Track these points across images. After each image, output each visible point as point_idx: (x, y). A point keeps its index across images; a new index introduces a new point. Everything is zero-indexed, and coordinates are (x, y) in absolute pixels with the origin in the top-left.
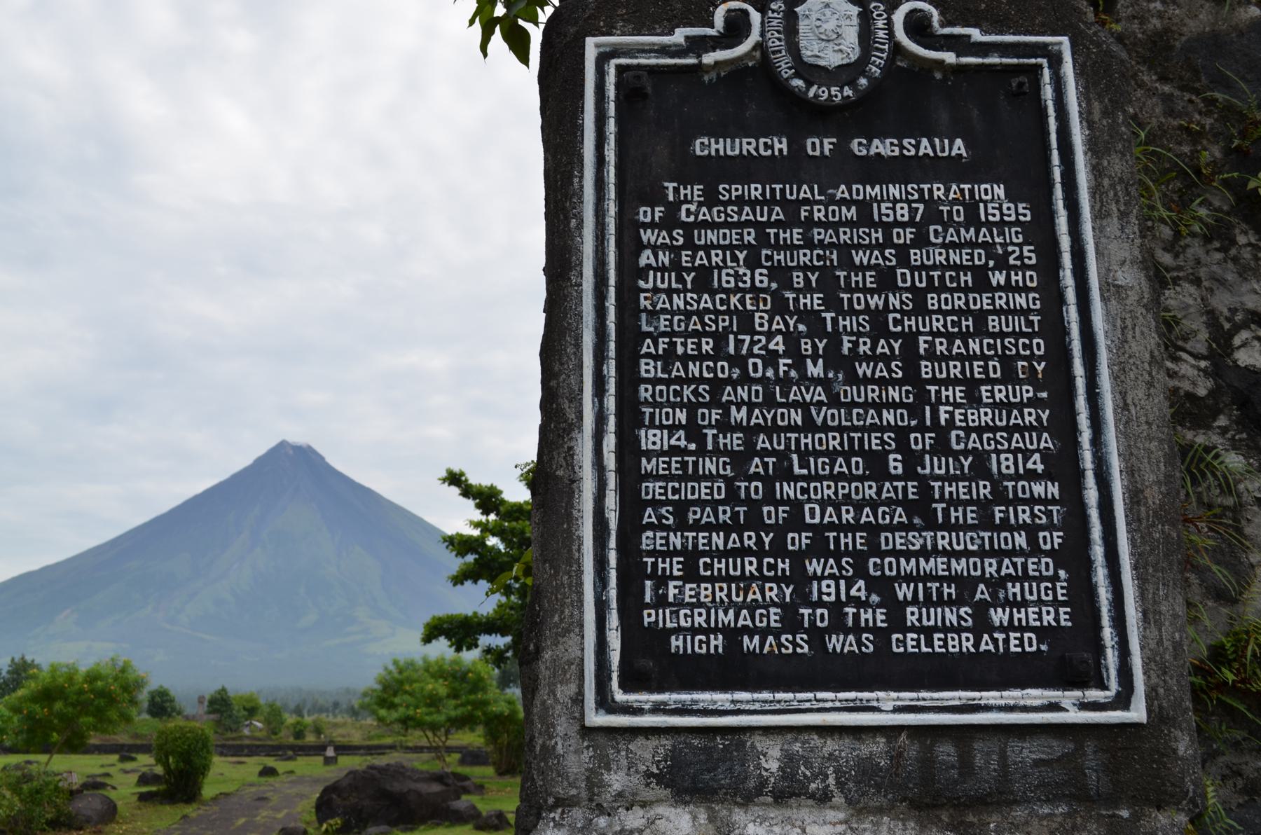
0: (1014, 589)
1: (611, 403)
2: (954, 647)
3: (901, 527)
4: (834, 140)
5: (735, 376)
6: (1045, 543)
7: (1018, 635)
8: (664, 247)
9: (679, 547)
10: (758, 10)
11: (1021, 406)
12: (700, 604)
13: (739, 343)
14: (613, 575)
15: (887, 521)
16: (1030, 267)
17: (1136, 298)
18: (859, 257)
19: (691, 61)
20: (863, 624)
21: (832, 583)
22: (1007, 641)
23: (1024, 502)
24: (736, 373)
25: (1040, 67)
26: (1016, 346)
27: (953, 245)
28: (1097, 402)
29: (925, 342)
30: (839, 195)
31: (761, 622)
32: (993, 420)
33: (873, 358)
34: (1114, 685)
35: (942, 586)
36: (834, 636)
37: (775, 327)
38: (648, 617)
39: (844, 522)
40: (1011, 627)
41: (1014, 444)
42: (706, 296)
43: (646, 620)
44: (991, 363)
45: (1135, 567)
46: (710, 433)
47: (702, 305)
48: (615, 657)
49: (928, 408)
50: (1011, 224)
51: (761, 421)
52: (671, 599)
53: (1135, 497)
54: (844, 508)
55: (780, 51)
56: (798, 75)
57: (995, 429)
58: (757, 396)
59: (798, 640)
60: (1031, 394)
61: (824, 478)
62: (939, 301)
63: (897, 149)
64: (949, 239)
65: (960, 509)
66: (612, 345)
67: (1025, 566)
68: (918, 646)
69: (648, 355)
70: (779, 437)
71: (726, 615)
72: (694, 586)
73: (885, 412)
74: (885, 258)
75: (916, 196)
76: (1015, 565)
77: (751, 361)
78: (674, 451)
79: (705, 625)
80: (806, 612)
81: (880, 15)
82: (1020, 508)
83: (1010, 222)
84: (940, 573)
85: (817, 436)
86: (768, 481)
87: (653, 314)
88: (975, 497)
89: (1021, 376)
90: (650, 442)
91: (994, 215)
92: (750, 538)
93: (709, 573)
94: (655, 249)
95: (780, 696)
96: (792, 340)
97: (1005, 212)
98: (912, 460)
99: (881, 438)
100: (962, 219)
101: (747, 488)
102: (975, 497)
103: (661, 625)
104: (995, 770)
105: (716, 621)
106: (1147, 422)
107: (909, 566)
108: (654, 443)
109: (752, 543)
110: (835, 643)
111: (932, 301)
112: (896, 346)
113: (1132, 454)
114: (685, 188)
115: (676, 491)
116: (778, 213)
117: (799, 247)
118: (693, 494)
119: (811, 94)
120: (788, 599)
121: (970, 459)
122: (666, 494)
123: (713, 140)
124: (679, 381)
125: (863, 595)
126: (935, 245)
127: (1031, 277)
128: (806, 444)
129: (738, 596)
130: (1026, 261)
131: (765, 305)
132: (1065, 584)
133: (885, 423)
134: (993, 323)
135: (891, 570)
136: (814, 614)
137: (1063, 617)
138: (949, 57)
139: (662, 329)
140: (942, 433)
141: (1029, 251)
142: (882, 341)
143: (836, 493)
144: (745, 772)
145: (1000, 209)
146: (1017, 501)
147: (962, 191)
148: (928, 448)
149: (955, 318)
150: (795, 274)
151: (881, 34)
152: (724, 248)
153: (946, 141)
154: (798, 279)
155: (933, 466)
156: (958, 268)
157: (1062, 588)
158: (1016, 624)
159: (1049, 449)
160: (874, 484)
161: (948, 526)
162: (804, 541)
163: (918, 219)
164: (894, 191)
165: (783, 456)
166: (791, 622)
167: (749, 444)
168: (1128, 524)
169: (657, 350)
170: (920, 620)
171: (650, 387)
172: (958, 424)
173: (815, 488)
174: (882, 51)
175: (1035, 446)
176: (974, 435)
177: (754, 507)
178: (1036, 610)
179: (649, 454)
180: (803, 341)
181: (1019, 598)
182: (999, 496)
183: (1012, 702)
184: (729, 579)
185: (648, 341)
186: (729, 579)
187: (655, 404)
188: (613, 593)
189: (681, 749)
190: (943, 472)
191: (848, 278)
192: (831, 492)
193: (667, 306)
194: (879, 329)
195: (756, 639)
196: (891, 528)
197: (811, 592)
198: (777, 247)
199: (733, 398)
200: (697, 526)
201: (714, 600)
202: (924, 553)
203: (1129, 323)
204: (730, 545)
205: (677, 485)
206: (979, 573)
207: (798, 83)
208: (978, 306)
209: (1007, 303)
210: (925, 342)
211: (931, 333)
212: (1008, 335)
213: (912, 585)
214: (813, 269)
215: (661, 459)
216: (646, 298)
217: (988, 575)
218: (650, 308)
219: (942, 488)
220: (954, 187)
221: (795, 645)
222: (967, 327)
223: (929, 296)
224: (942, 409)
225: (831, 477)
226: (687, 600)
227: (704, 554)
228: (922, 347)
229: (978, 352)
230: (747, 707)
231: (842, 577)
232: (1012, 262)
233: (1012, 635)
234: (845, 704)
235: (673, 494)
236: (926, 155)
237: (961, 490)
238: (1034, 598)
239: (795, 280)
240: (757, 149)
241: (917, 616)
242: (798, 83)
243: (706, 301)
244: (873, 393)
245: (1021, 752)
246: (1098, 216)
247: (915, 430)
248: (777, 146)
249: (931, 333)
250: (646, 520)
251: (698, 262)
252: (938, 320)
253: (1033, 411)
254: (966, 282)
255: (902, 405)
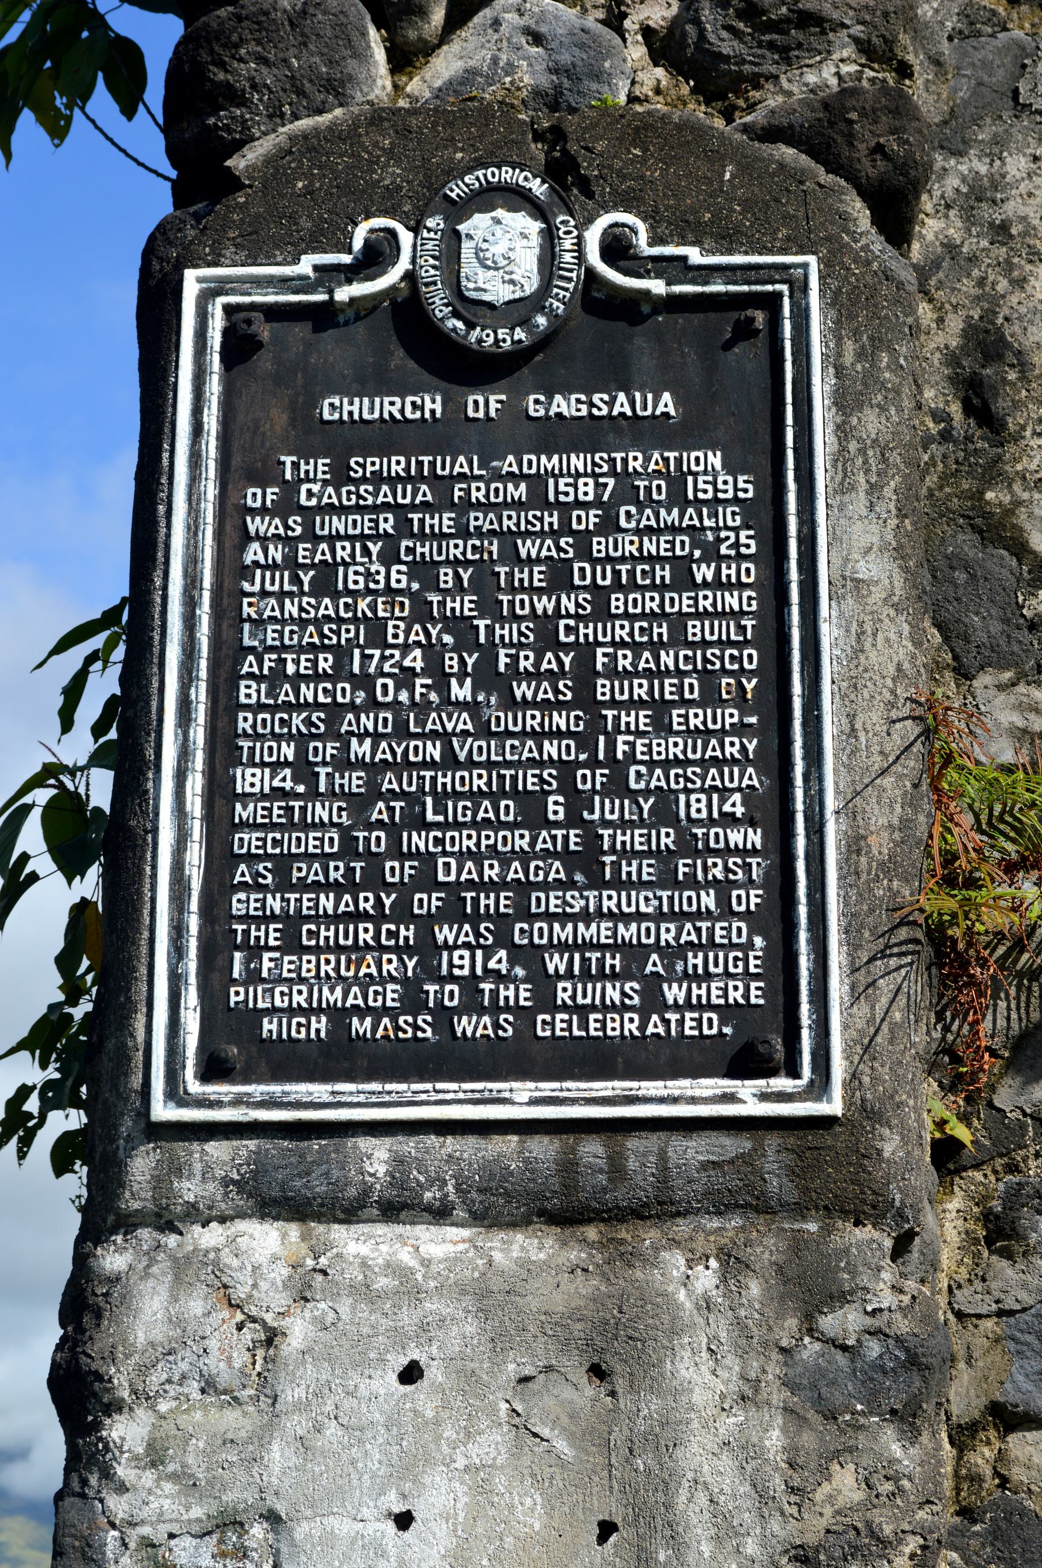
1: (199, 735)
4: (503, 397)
5: (358, 701)
7: (696, 1015)
9: (277, 911)
12: (302, 980)
13: (366, 658)
18: (527, 548)
19: (321, 297)
20: (502, 1003)
21: (466, 954)
22: (681, 1022)
23: (716, 852)
24: (360, 697)
25: (779, 295)
26: (722, 659)
29: (605, 655)
30: (506, 469)
33: (535, 676)
36: (465, 1018)
37: (412, 638)
40: (689, 1005)
41: (709, 782)
42: (327, 601)
43: (233, 999)
44: (687, 681)
46: (323, 771)
49: (602, 738)
54: (486, 863)
58: (385, 726)
59: (420, 1022)
60: (735, 720)
64: (644, 522)
65: (635, 863)
66: (203, 664)
67: (711, 931)
68: (570, 1029)
69: (251, 676)
70: (410, 777)
72: (294, 958)
73: (546, 743)
74: (559, 549)
75: (605, 468)
77: (380, 681)
78: (279, 793)
80: (431, 988)
83: (726, 501)
84: (603, 940)
85: (458, 774)
86: (393, 830)
89: (725, 696)
94: (264, 540)
96: (433, 653)
97: (720, 486)
98: (577, 802)
99: (540, 777)
100: (663, 497)
101: (367, 839)
106: (881, 753)
107: (564, 933)
108: (252, 785)
109: (368, 906)
110: (464, 1025)
111: (617, 603)
112: (567, 661)
116: (426, 493)
117: (451, 536)
120: (410, 974)
121: (651, 801)
123: (346, 400)
124: (288, 707)
125: (504, 968)
126: (626, 531)
127: (748, 570)
128: (444, 785)
129: (348, 969)
130: (743, 550)
131: (402, 610)
134: (694, 630)
135: (541, 937)
137: (753, 992)
139: (269, 642)
140: (617, 768)
142: (549, 655)
143: (478, 845)
145: (714, 484)
147: (666, 460)
148: (598, 787)
150: (442, 571)
153: (650, 396)
154: (446, 577)
155: (604, 809)
156: (651, 559)
157: (756, 958)
158: (694, 1001)
160: (526, 833)
161: (618, 884)
162: (435, 903)
163: (605, 498)
164: (577, 462)
165: (414, 800)
166: (413, 1000)
169: (261, 668)
170: (573, 997)
171: (250, 716)
172: (639, 757)
173: (453, 838)
174: (569, 280)
175: (735, 784)
176: (658, 771)
177: (375, 861)
178: (722, 985)
180: (447, 655)
181: (700, 971)
184: (339, 949)
185: (251, 658)
186: (339, 949)
187: (257, 737)
190: (615, 816)
191: (510, 575)
192: (471, 843)
194: (547, 639)
195: (368, 1020)
196: (545, 886)
198: (422, 537)
199: (354, 728)
200: (303, 886)
201: (318, 976)
202: (585, 916)
203: (868, 628)
204: (342, 908)
205: (278, 836)
208: (676, 609)
210: (605, 655)
211: (613, 643)
214: (467, 563)
216: (250, 605)
217: (663, 943)
218: (254, 616)
220: (656, 455)
222: (660, 635)
224: (621, 739)
225: (474, 824)
226: (285, 974)
227: (308, 919)
228: (600, 660)
229: (672, 668)
231: (480, 946)
233: (688, 1015)
234: (470, 1095)
236: (622, 415)
238: (720, 970)
239: (442, 578)
240: (402, 411)
241: (570, 992)
244: (533, 720)
246: (843, 488)
248: (428, 405)
249: (613, 643)
250: (238, 879)
251: (318, 557)
252: (622, 627)
253: (736, 740)
254: (663, 577)
255: (570, 734)
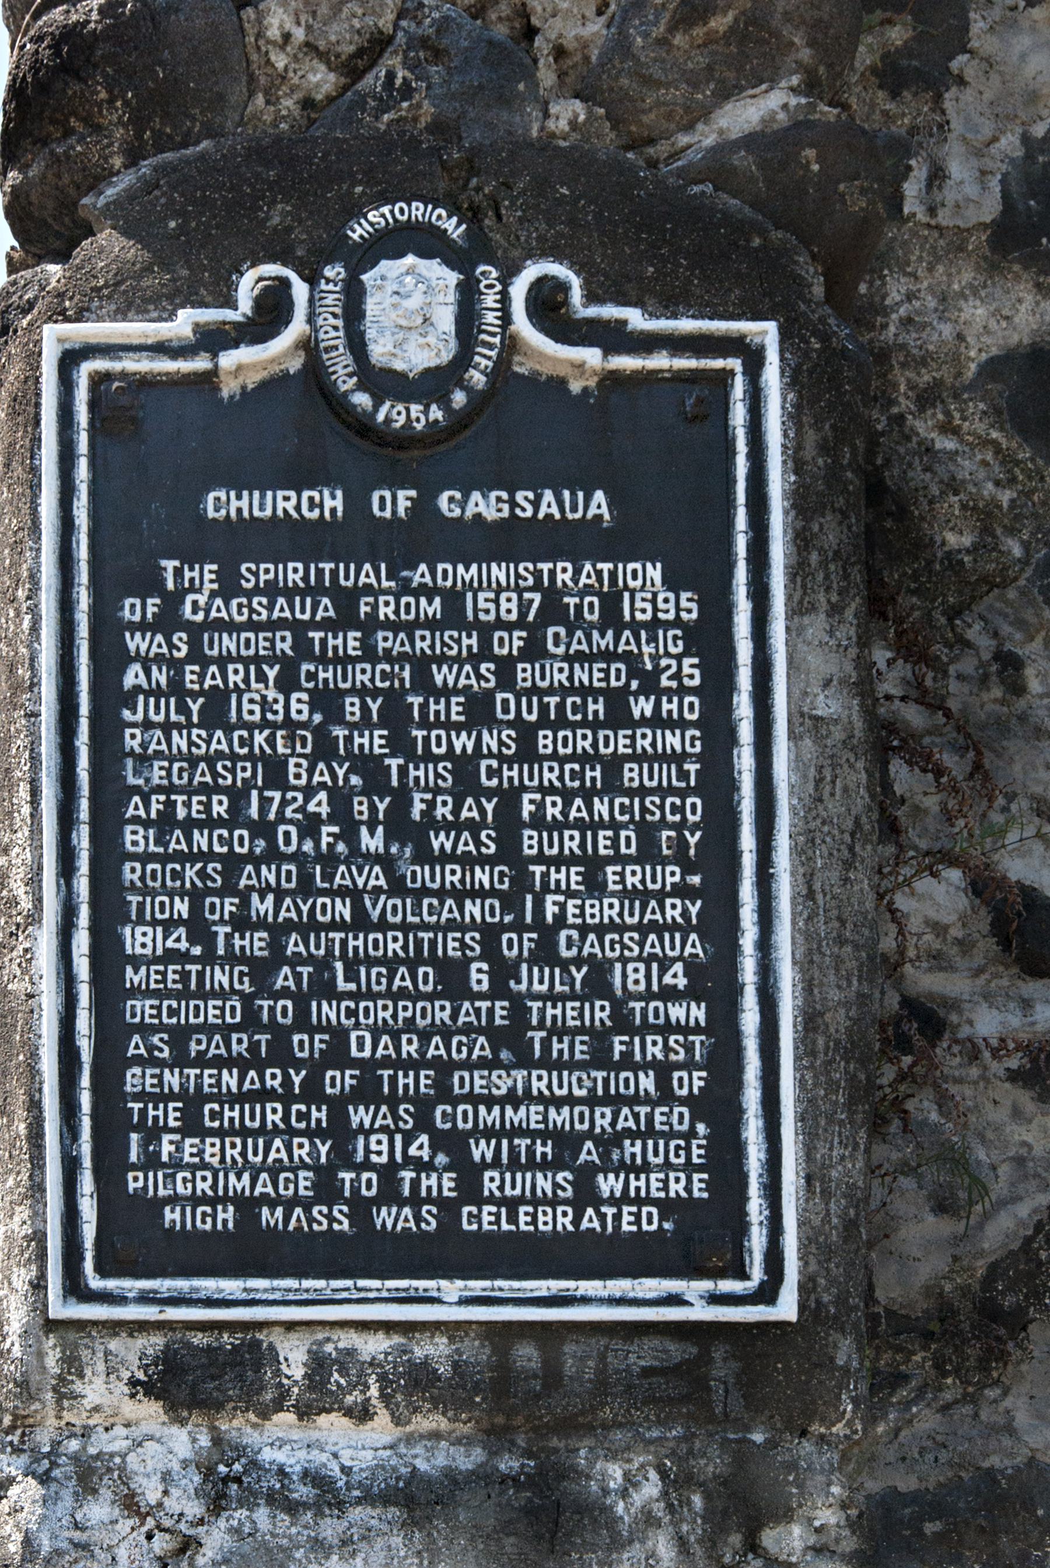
0: (633, 1149)
1: (82, 886)
2: (545, 1223)
3: (484, 1064)
5: (258, 850)
6: (681, 1087)
7: (634, 1209)
8: (159, 659)
9: (176, 1089)
10: (304, 279)
11: (661, 896)
12: (205, 1166)
13: (265, 803)
14: (86, 1123)
15: (464, 1055)
16: (692, 691)
17: (843, 736)
20: (424, 1194)
22: (617, 1217)
24: (261, 844)
26: (662, 807)
27: (580, 657)
28: (770, 888)
30: (417, 580)
31: (286, 1188)
32: (621, 915)
33: (455, 826)
34: (757, 1273)
35: (534, 1143)
36: (384, 1210)
37: (316, 779)
38: (134, 1182)
39: (404, 1055)
42: (219, 733)
43: (132, 1186)
44: (623, 834)
45: (801, 1118)
46: (222, 930)
47: (214, 746)
48: (89, 1232)
49: (529, 898)
50: (667, 625)
51: (293, 915)
52: (165, 1158)
53: (810, 1021)
54: (404, 1038)
55: (336, 348)
56: (361, 387)
57: (622, 929)
58: (289, 880)
59: (336, 1213)
60: (677, 878)
61: (379, 995)
62: (555, 742)
63: (506, 507)
64: (574, 647)
65: (566, 1039)
67: (650, 1118)
68: (498, 1222)
69: (136, 820)
70: (318, 938)
71: (239, 1178)
72: (197, 1141)
74: (479, 677)
76: (636, 1116)
77: (282, 829)
78: (171, 956)
79: (210, 1193)
81: (490, 286)
82: (649, 1039)
83: (667, 621)
85: (371, 937)
86: (301, 1001)
87: (144, 760)
88: (587, 1023)
90: (137, 944)
91: (644, 611)
92: (274, 1076)
93: (216, 1124)
95: (307, 1283)
97: (661, 605)
98: (503, 972)
99: (462, 941)
102: (587, 1023)
103: (151, 1192)
104: (590, 1381)
105: (226, 1188)
106: (839, 919)
107: (490, 1117)
108: (144, 945)
109: (276, 1084)
110: (385, 1217)
111: (545, 741)
112: (489, 807)
113: (811, 962)
114: (192, 569)
115: (173, 1012)
117: (355, 660)
118: (197, 1016)
119: (381, 417)
120: (323, 1160)
121: (585, 969)
122: (159, 1016)
124: (180, 857)
125: (425, 1154)
126: (554, 656)
127: (691, 705)
131: (304, 746)
132: (704, 1142)
133: (468, 919)
134: (631, 774)
136: (358, 1179)
138: (592, 356)
139: (156, 781)
141: (692, 666)
142: (470, 800)
143: (395, 1016)
144: (261, 1380)
145: (654, 601)
146: (646, 1028)
147: (599, 573)
148: (526, 953)
149: (577, 767)
150: (348, 700)
151: (491, 317)
152: (246, 661)
153: (581, 495)
154: (352, 708)
155: (532, 980)
157: (699, 1147)
158: (632, 1194)
159: (697, 955)
162: (348, 1081)
163: (531, 618)
164: (499, 572)
165: (323, 965)
166: (326, 1189)
167: (276, 946)
168: (797, 1058)
169: (148, 812)
170: (501, 1188)
171: (138, 866)
173: (367, 1009)
176: (592, 937)
177: (280, 1035)
178: (662, 1176)
179: (136, 962)
180: (356, 800)
181: (639, 1161)
182: (622, 1022)
183: (618, 1295)
184: (244, 1132)
185: (136, 799)
186: (244, 1132)
188: (86, 1148)
189: (176, 1351)
190: (545, 987)
192: (388, 1014)
193: (164, 747)
195: (279, 1211)
196: (468, 1065)
197: (355, 1150)
198: (323, 660)
200: (202, 1061)
202: (512, 1099)
203: (828, 774)
205: (175, 1004)
206: (586, 1126)
207: (362, 400)
209: (653, 744)
210: (531, 802)
212: (651, 791)
213: (493, 1142)
214: (375, 693)
215: (153, 968)
217: (598, 1130)
218: (138, 750)
219: (542, 1011)
220: (588, 567)
221: (331, 1219)
222: (593, 779)
223: (541, 733)
224: (550, 898)
225: (389, 994)
226: (187, 1159)
227: (211, 1098)
228: (527, 809)
229: (606, 817)
230: (264, 1297)
231: (398, 1130)
232: (665, 682)
233: (626, 1209)
235: (170, 1016)
236: (549, 516)
237: (570, 1013)
238: (660, 1160)
239: (348, 709)
240: (298, 508)
241: (497, 1183)
242: (362, 400)
243: (219, 742)
245: (626, 1358)
246: (796, 610)
247: (509, 928)
248: (328, 504)
250: (131, 1051)
251: (208, 683)
253: (678, 902)
255: (493, 892)
